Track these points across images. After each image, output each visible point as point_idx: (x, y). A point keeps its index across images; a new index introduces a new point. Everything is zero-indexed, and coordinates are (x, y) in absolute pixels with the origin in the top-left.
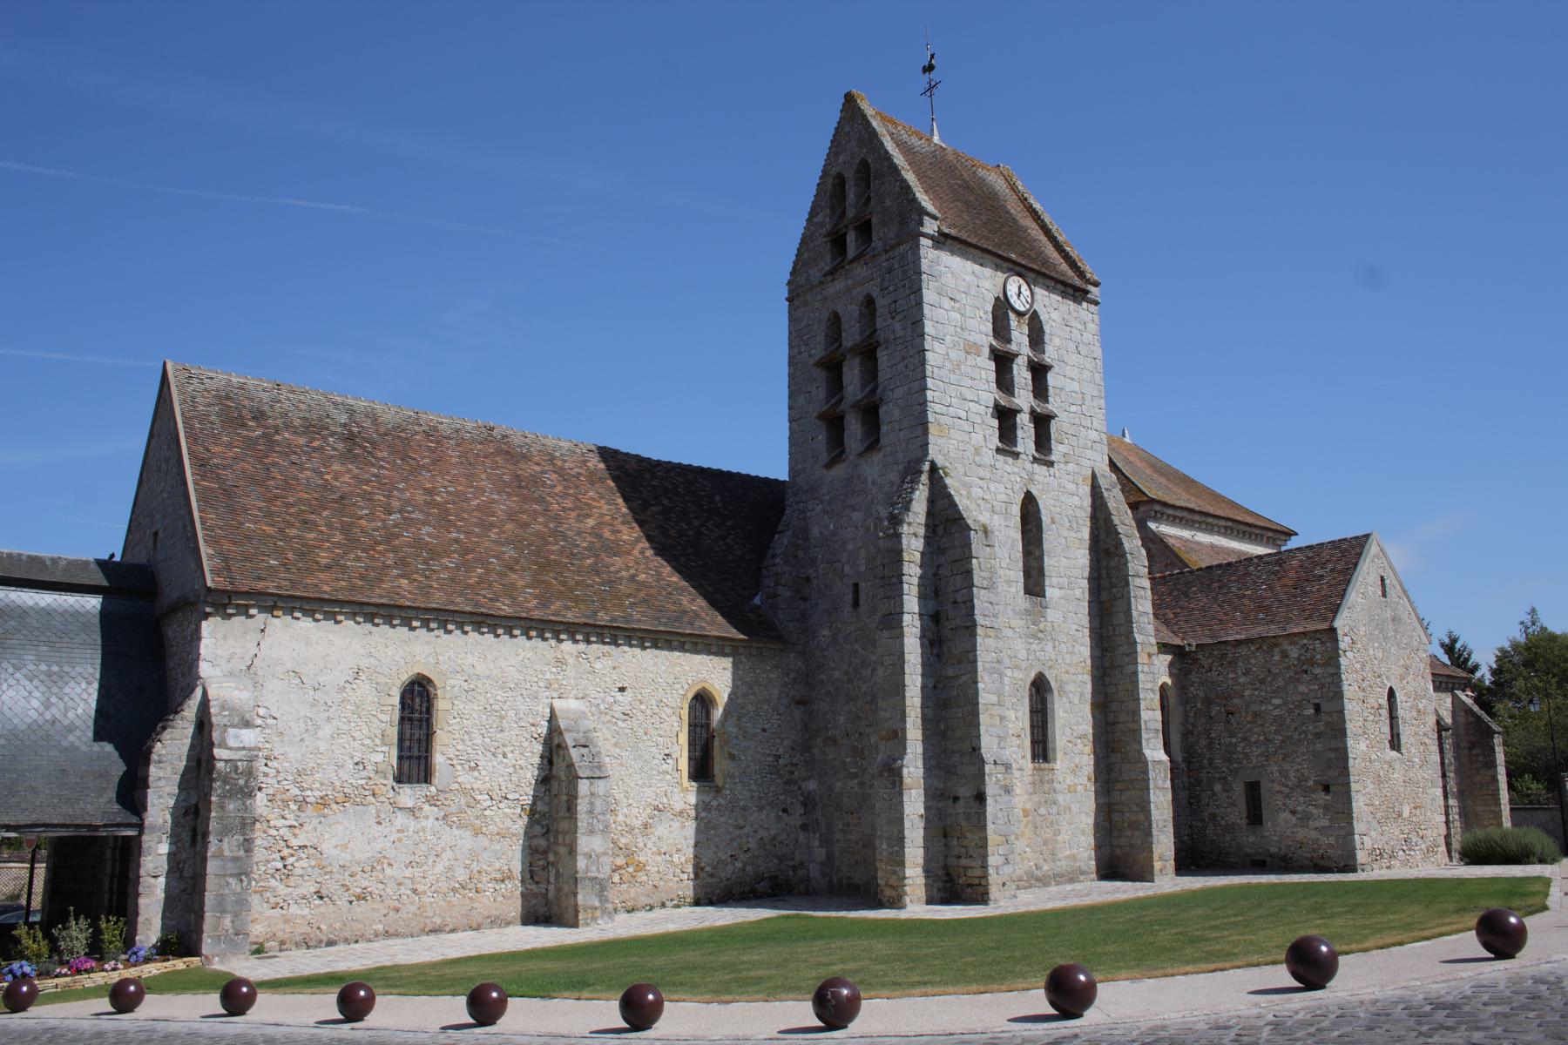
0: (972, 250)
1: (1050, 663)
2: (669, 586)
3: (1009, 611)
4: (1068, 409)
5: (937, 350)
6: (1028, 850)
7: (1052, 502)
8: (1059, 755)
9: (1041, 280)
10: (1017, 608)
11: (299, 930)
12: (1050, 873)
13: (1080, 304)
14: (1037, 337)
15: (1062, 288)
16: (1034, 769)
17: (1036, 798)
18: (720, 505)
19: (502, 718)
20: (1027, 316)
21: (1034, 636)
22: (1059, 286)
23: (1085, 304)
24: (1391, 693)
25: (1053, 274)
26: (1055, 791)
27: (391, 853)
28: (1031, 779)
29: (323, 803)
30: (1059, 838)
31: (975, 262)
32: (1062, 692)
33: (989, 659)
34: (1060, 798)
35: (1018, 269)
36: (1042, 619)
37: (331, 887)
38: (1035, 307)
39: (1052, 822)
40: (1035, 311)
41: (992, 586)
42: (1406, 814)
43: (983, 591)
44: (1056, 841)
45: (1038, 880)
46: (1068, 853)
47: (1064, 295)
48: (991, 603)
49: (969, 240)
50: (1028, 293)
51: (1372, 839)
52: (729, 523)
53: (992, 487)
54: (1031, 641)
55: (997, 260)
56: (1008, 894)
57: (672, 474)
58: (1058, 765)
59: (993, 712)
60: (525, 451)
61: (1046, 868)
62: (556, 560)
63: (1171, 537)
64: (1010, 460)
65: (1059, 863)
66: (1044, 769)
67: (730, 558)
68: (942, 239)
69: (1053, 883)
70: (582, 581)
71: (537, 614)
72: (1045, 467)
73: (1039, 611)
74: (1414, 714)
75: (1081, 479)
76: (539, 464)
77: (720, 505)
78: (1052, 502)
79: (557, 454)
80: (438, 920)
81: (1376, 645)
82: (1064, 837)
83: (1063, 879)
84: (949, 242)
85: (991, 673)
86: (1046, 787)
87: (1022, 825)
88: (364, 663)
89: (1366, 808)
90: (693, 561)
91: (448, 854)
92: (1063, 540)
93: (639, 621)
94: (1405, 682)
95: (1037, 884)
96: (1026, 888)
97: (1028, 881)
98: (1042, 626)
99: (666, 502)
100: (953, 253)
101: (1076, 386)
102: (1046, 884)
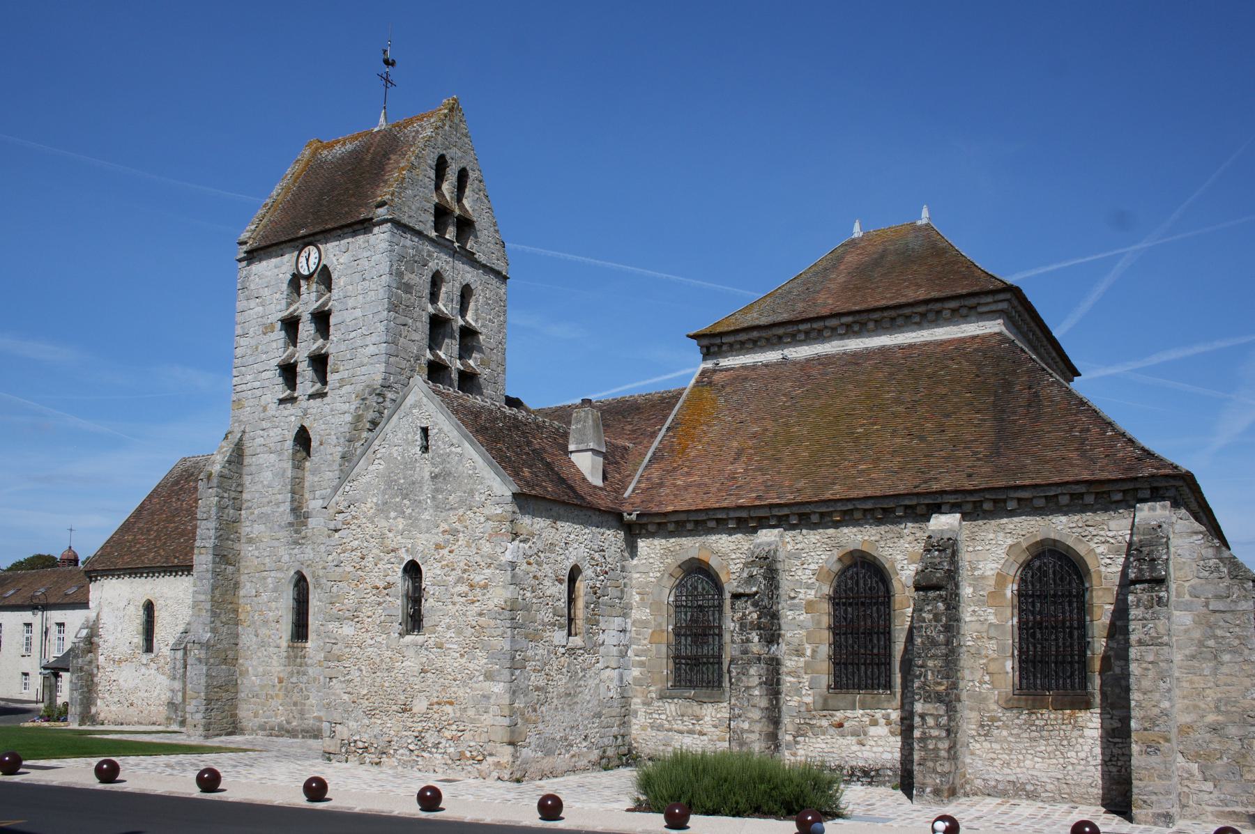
0: (270, 249)
1: (309, 562)
3: (276, 527)
4: (347, 337)
5: (242, 344)
6: (280, 708)
7: (323, 427)
8: (311, 636)
9: (329, 236)
10: (283, 524)
11: (113, 717)
12: (299, 728)
13: (371, 232)
15: (351, 230)
16: (289, 647)
17: (289, 668)
19: (177, 618)
20: (315, 276)
21: (296, 543)
22: (346, 230)
23: (376, 230)
24: (413, 570)
26: (306, 665)
27: (140, 685)
28: (285, 654)
29: (120, 661)
30: (308, 702)
31: (277, 256)
32: (318, 585)
33: (201, 569)
34: (310, 671)
35: (306, 240)
36: (304, 528)
37: (123, 700)
38: (324, 262)
39: (302, 689)
40: (325, 267)
41: (210, 517)
42: (420, 706)
43: (204, 522)
44: (305, 704)
45: (288, 731)
46: (315, 714)
47: (355, 233)
48: (208, 529)
51: (349, 730)
53: (272, 433)
54: (293, 547)
55: (289, 244)
56: (198, 733)
58: (309, 644)
59: (201, 607)
61: (294, 724)
64: (289, 405)
65: (306, 722)
66: (297, 647)
68: (251, 256)
69: (300, 736)
72: (320, 399)
73: (302, 522)
74: (465, 588)
75: (354, 396)
78: (323, 427)
80: (154, 719)
81: (393, 514)
82: (312, 701)
83: (308, 735)
84: (255, 254)
85: (202, 580)
86: (299, 660)
87: (277, 688)
88: (131, 596)
89: (346, 697)
91: (158, 687)
92: (328, 457)
94: (445, 552)
95: (287, 735)
96: (277, 736)
97: (279, 731)
98: (303, 533)
100: (260, 260)
101: (358, 313)
102: (295, 736)
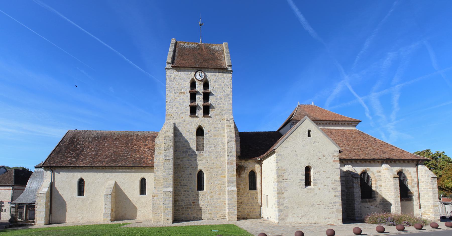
14: (206, 85)
50: (203, 74)
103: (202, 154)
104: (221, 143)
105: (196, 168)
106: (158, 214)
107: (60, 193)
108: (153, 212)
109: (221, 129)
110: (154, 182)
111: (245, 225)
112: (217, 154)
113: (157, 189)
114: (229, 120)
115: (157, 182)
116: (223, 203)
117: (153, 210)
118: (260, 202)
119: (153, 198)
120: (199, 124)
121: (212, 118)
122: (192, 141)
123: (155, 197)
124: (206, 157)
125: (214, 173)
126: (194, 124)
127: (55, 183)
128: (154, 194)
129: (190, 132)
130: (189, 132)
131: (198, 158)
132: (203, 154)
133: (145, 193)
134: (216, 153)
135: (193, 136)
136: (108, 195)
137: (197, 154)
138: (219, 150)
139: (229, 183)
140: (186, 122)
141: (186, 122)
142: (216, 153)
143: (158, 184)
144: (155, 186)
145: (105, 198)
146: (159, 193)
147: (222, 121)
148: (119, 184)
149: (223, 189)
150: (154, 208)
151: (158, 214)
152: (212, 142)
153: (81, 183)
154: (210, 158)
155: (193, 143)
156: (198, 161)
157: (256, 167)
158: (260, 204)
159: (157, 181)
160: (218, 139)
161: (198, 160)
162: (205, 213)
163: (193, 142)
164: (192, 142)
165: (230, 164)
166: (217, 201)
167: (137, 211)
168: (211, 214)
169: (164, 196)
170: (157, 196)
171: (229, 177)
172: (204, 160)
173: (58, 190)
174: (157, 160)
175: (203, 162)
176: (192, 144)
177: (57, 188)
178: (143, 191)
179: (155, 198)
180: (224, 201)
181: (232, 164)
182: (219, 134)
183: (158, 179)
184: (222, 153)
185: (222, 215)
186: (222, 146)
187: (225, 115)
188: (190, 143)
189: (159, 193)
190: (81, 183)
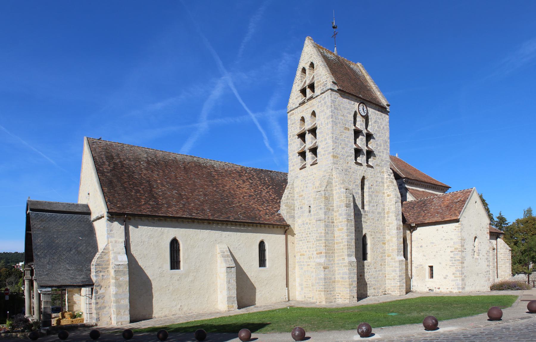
2: (252, 208)
18: (267, 181)
25: (374, 102)
49: (346, 91)
52: (270, 187)
57: (252, 172)
60: (205, 165)
62: (216, 200)
63: (410, 189)
67: (271, 198)
70: (225, 207)
71: (211, 218)
76: (209, 169)
77: (267, 181)
79: (215, 166)
90: (259, 200)
93: (242, 219)
99: (251, 181)
103: (367, 214)
104: (381, 202)
105: (362, 231)
106: (330, 291)
107: (140, 263)
108: (325, 290)
109: (381, 184)
110: (325, 249)
111: (364, 302)
112: (379, 215)
113: (328, 258)
114: (390, 174)
115: (328, 249)
116: (384, 275)
117: (325, 287)
118: (410, 273)
119: (324, 271)
120: (363, 175)
121: (374, 169)
122: (357, 195)
123: (326, 269)
124: (369, 219)
125: (377, 239)
126: (359, 174)
127: (131, 245)
128: (325, 265)
129: (356, 184)
130: (355, 184)
131: (363, 219)
132: (367, 215)
133: (177, 267)
134: (378, 214)
135: (358, 189)
136: (232, 267)
137: (362, 213)
138: (380, 211)
139: (398, 251)
140: (352, 170)
141: (352, 170)
142: (378, 214)
143: (329, 251)
144: (326, 255)
145: (227, 272)
146: (329, 263)
147: (382, 174)
148: (232, 249)
149: (384, 258)
150: (326, 284)
151: (330, 291)
152: (375, 199)
153: (174, 245)
154: (373, 219)
155: (359, 199)
156: (363, 223)
157: (407, 233)
158: (410, 276)
159: (328, 248)
160: (379, 196)
161: (363, 222)
162: (370, 288)
163: (359, 198)
164: (358, 197)
165: (398, 229)
166: (379, 274)
167: (255, 292)
168: (374, 289)
169: (350, 267)
170: (329, 268)
171: (398, 245)
172: (368, 221)
173: (137, 259)
174: (327, 219)
175: (367, 224)
176: (357, 200)
177: (134, 255)
178: (262, 262)
179: (326, 270)
180: (385, 273)
181: (400, 229)
182: (380, 190)
183: (329, 245)
184: (382, 215)
185: (384, 290)
186: (382, 205)
187: (384, 166)
188: (356, 198)
189: (329, 263)
190: (174, 245)
